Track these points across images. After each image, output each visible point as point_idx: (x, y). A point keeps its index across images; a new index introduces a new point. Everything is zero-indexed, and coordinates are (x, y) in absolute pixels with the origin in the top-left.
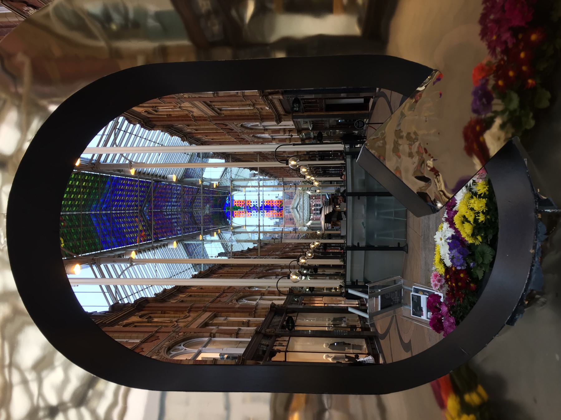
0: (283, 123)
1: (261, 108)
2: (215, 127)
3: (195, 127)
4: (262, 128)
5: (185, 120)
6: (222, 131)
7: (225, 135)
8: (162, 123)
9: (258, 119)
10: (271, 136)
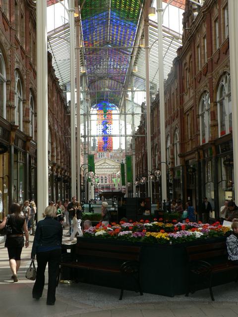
0: (178, 158)
1: (189, 144)
3: (175, 94)
5: (180, 89)
9: (182, 141)
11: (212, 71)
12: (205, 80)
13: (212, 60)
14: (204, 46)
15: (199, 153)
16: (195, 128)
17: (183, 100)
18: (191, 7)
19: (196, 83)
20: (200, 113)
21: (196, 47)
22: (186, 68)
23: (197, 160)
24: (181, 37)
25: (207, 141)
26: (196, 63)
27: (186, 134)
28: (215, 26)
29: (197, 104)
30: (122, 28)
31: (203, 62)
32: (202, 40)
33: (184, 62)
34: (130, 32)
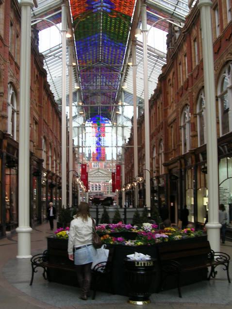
0: (163, 167)
3: (160, 107)
4: (160, 152)
6: (158, 125)
14: (185, 63)
15: (181, 162)
20: (182, 124)
21: (178, 64)
23: (179, 168)
25: (188, 151)
27: (170, 144)
29: (179, 116)
30: (113, 48)
34: (120, 52)
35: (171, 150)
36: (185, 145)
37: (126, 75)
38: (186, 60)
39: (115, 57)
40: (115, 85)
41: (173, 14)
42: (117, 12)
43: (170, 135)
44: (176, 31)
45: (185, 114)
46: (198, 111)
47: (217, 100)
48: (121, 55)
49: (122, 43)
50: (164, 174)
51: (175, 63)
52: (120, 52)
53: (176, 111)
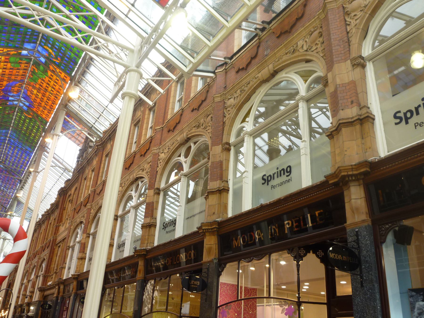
1: (52, 278)
2: (49, 239)
3: (52, 224)
4: (39, 274)
5: (58, 219)
6: (45, 243)
7: (41, 244)
8: (61, 202)
9: (46, 273)
10: (31, 280)
11: (93, 202)
12: (84, 211)
13: (95, 191)
14: (91, 178)
15: (59, 288)
16: (63, 259)
17: (58, 230)
18: (88, 144)
19: (74, 213)
20: (71, 244)
21: (83, 179)
22: (69, 200)
23: (55, 295)
24: (73, 170)
25: (70, 276)
26: (80, 194)
27: (52, 266)
28: (105, 160)
29: (70, 234)
30: (18, 151)
31: (86, 193)
32: (90, 173)
33: (69, 193)
34: (26, 157)
35: (52, 273)
36: (69, 268)
37: (25, 183)
38: (92, 175)
39: (18, 161)
40: (10, 192)
41: (91, 128)
42: (34, 113)
43: (55, 255)
44: (91, 147)
45: (77, 233)
46: (92, 231)
47: (116, 219)
48: (26, 160)
49: (30, 147)
50: (37, 301)
51: (80, 177)
52: (26, 157)
53: (69, 229)
